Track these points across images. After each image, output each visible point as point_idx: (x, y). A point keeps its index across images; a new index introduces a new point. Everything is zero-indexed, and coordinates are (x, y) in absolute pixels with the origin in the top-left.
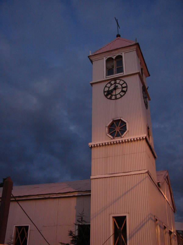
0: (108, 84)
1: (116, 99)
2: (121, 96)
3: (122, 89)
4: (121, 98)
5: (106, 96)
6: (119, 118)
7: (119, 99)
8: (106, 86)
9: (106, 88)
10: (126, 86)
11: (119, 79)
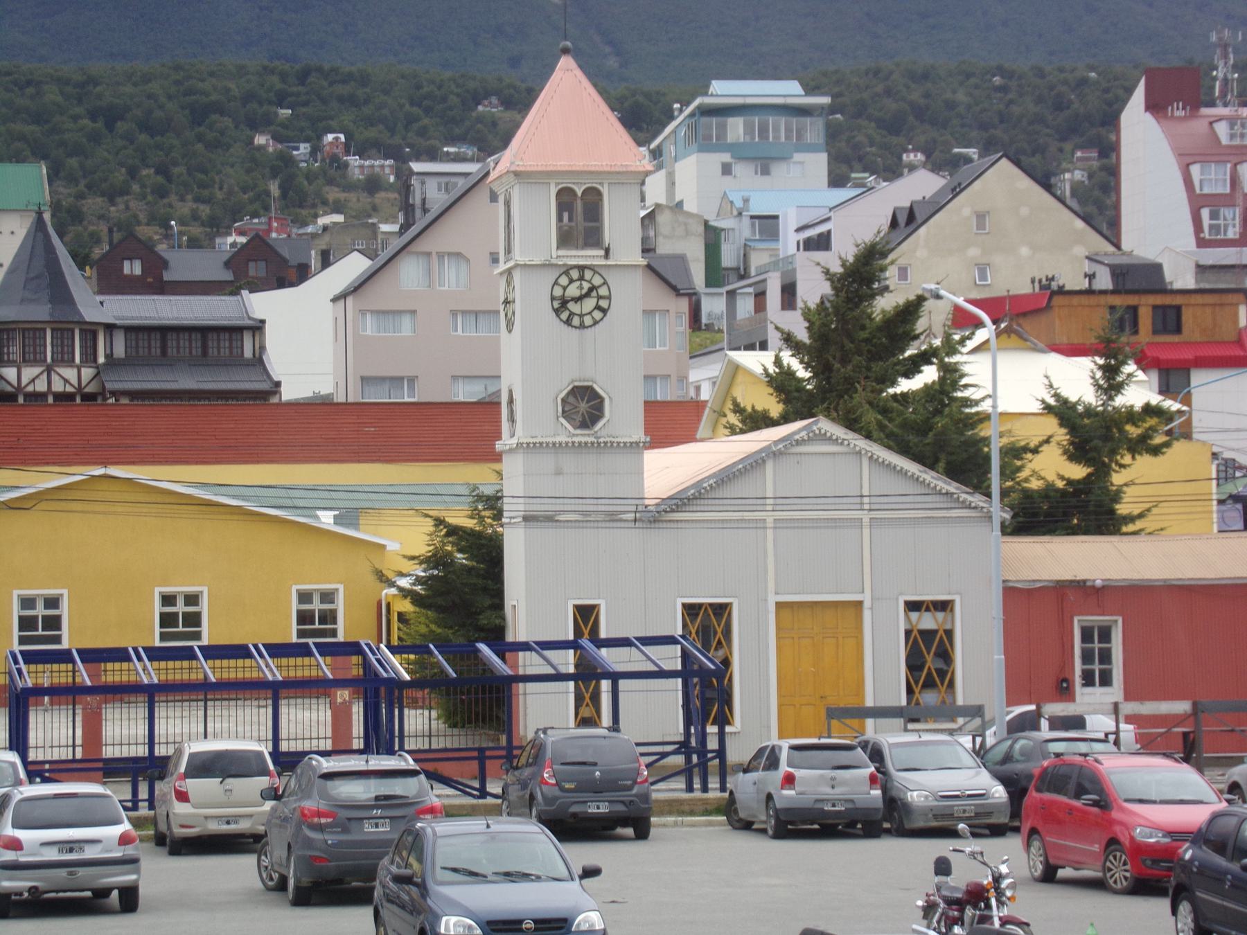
1: (582, 326)
2: (596, 323)
4: (593, 328)
5: (557, 312)
7: (589, 329)
8: (556, 283)
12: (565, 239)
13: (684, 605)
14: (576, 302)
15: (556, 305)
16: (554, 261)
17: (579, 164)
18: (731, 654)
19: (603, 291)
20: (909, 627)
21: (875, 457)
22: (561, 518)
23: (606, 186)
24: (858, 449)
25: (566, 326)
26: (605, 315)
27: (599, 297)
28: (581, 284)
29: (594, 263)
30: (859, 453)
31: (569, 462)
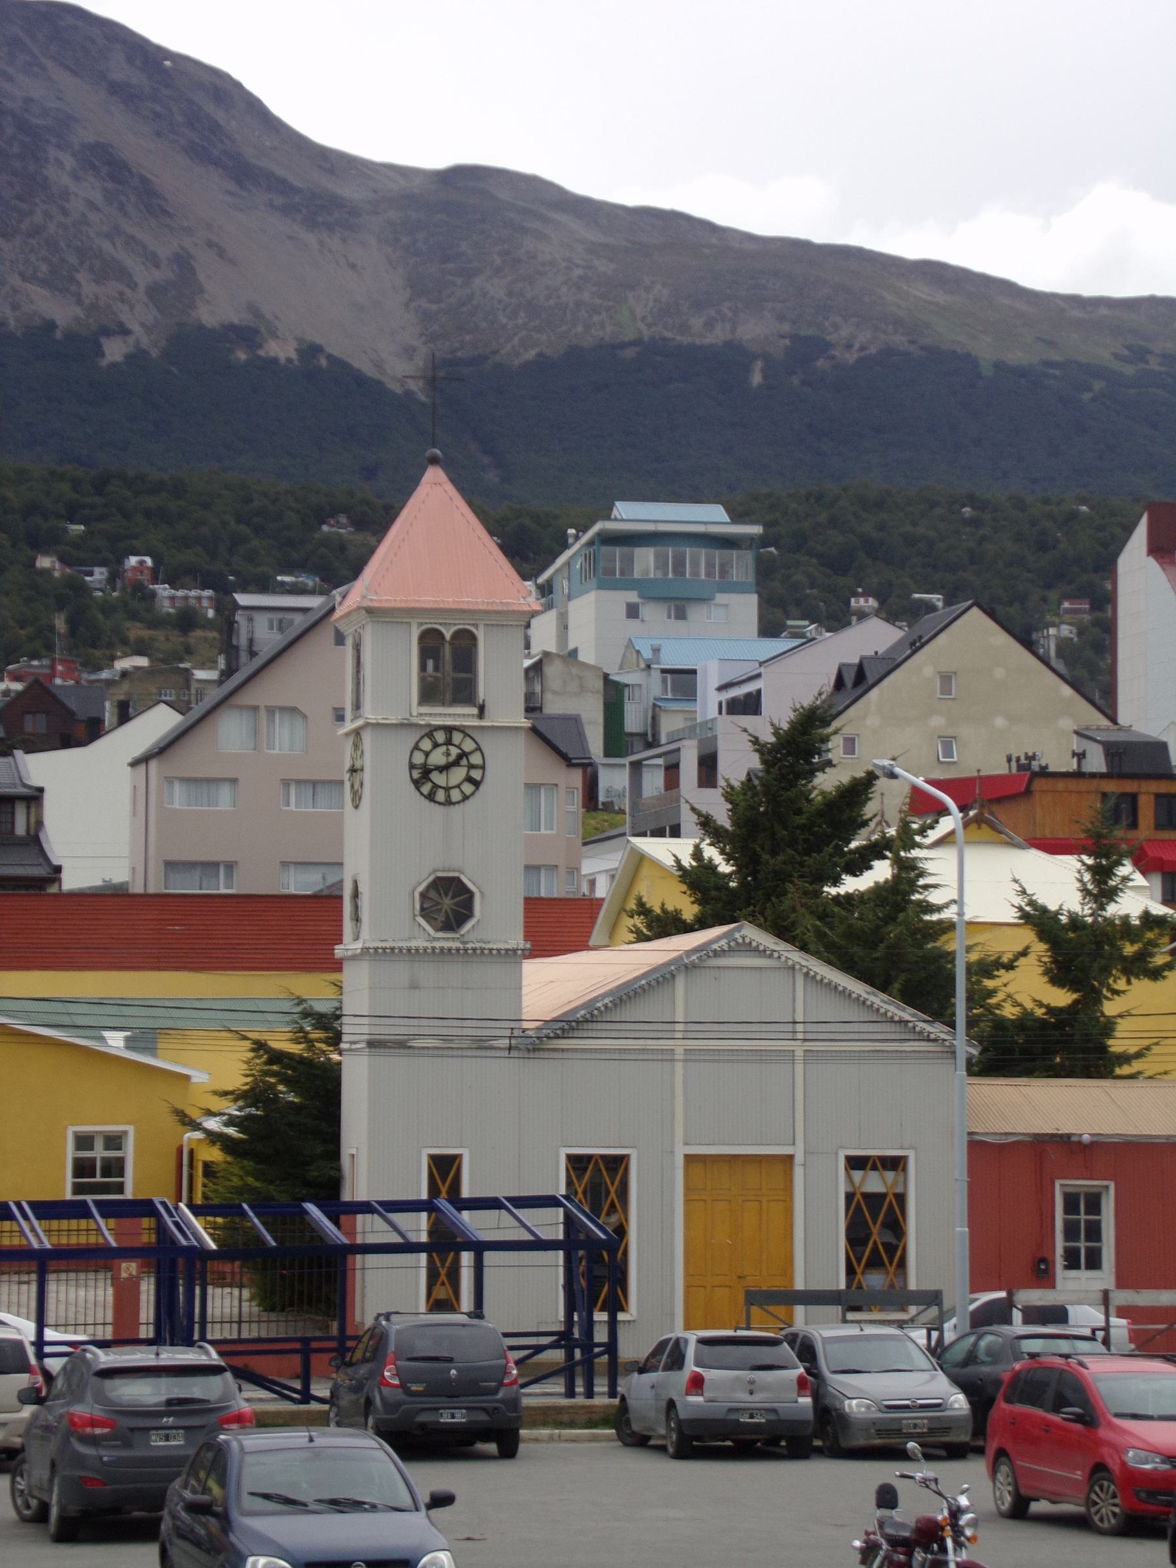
0: (422, 738)
1: (449, 802)
2: (466, 798)
5: (417, 784)
6: (456, 874)
8: (416, 747)
12: (429, 694)
14: (441, 772)
15: (416, 774)
16: (415, 720)
17: (449, 601)
18: (626, 1220)
19: (476, 759)
20: (850, 1190)
21: (812, 973)
23: (481, 628)
24: (790, 963)
25: (427, 801)
27: (471, 767)
28: (448, 750)
29: (464, 723)
30: (793, 968)
31: (427, 972)
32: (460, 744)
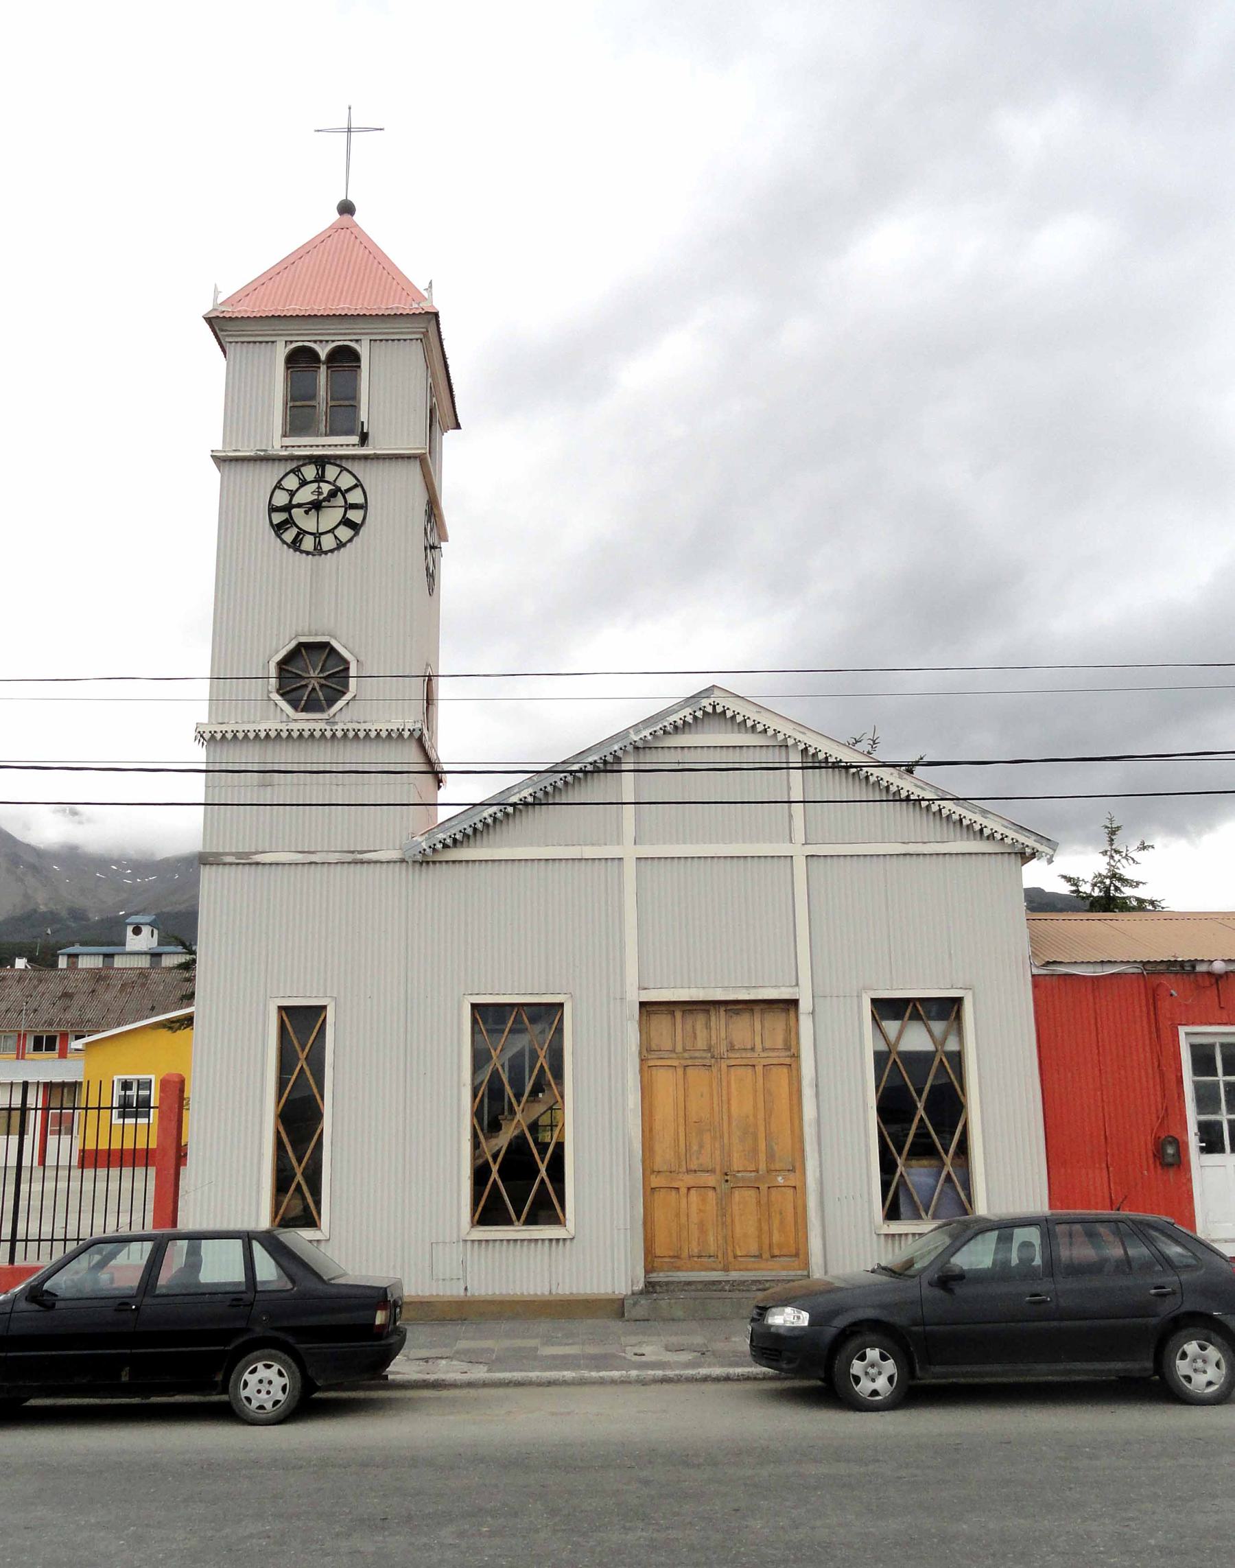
1: (318, 550)
2: (341, 545)
3: (345, 512)
5: (279, 528)
8: (278, 486)
9: (278, 492)
10: (361, 500)
11: (338, 462)
12: (298, 421)
13: (474, 1006)
19: (355, 497)
20: (883, 1047)
21: (811, 751)
22: (258, 858)
26: (357, 534)
28: (319, 487)
32: (335, 481)
